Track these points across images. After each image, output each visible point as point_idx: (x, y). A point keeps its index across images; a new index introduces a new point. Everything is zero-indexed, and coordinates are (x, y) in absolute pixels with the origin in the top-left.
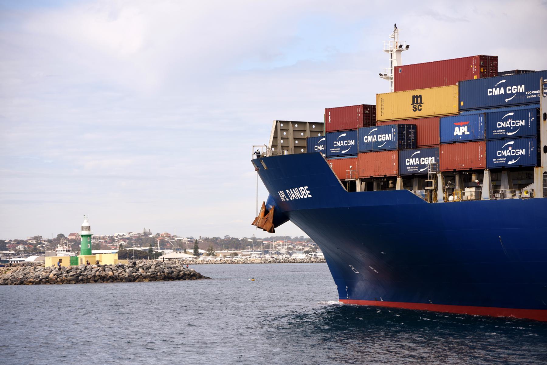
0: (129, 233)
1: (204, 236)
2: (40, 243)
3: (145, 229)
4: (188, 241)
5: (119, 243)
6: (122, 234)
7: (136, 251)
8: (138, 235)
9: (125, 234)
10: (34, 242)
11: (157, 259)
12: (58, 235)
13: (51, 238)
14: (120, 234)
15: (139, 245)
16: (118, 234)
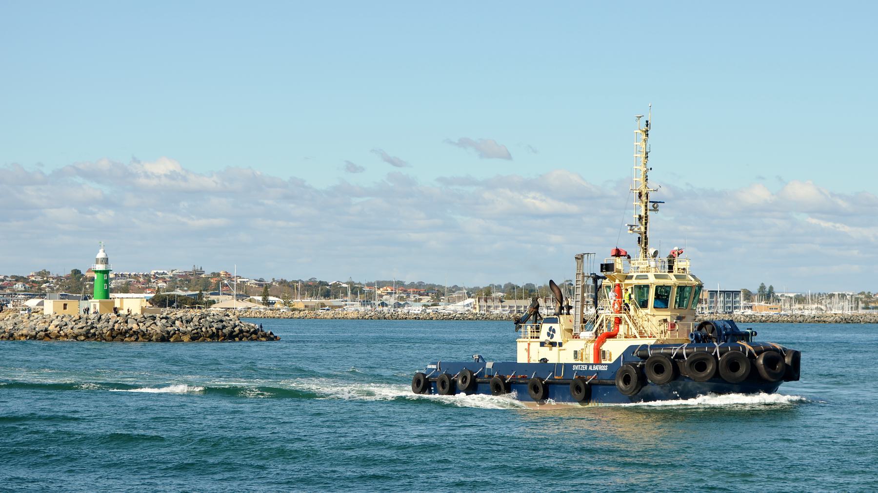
0: (172, 271)
1: (278, 278)
2: (47, 282)
3: (194, 266)
4: (256, 284)
5: (157, 283)
6: (162, 272)
7: (179, 296)
8: (184, 274)
9: (166, 272)
10: (39, 279)
11: (209, 308)
12: (72, 271)
13: (63, 274)
14: (159, 272)
15: (186, 289)
16: (156, 272)
